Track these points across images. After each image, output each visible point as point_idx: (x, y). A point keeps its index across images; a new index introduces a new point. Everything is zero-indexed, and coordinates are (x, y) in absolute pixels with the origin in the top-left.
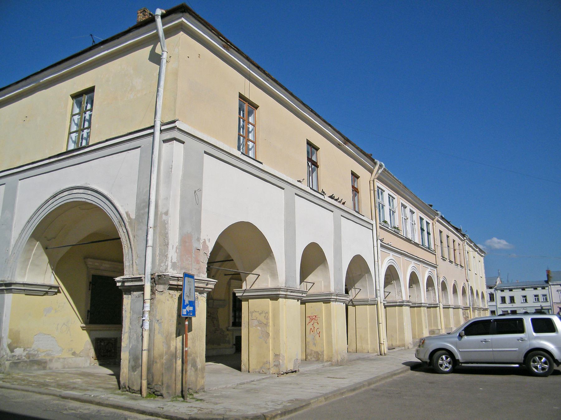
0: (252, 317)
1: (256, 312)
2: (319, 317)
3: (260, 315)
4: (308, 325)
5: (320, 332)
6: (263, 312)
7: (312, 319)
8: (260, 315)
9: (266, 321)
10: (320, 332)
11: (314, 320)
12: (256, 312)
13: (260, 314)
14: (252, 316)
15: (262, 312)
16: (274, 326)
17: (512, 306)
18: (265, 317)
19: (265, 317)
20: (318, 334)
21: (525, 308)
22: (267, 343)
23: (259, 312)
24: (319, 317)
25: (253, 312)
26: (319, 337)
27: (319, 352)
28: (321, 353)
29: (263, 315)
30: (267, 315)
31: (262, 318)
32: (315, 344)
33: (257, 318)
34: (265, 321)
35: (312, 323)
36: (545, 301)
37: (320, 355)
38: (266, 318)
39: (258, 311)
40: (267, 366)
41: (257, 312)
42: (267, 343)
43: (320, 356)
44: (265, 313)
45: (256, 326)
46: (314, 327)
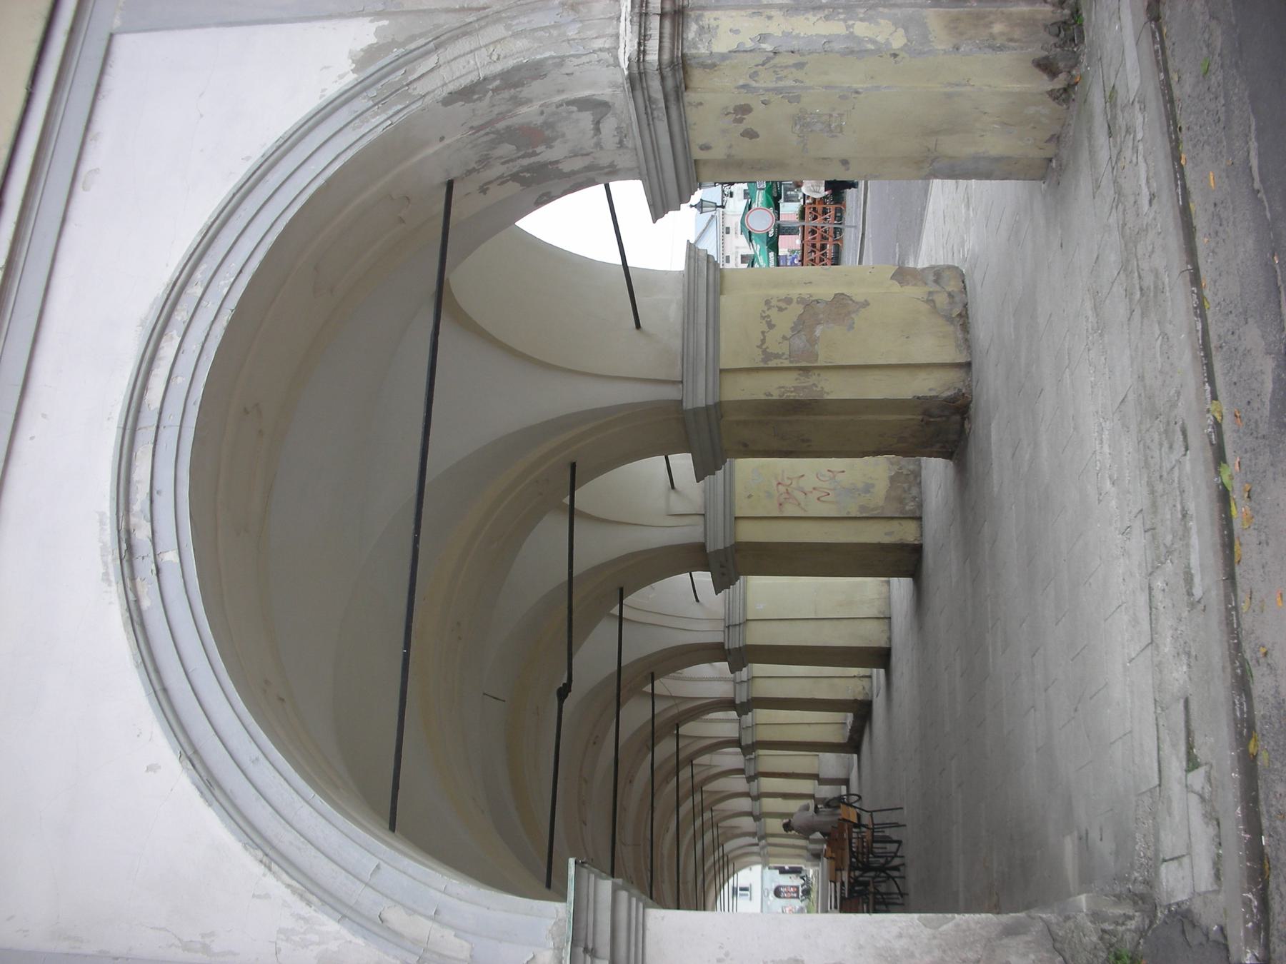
0: (783, 354)
1: (763, 341)
2: (783, 471)
3: (774, 326)
4: (805, 511)
5: (829, 471)
6: (764, 315)
7: (787, 496)
8: (774, 326)
9: (794, 304)
10: (829, 471)
11: (790, 490)
12: (763, 341)
13: (771, 326)
14: (777, 356)
15: (763, 318)
16: (810, 283)
18: (781, 309)
19: (781, 309)
20: (834, 476)
21: (766, 894)
22: (866, 301)
23: (765, 328)
24: (783, 471)
25: (764, 351)
26: (843, 472)
27: (893, 474)
28: (896, 468)
29: (773, 313)
30: (774, 302)
31: (784, 322)
32: (868, 488)
33: (784, 338)
34: (796, 310)
35: (800, 496)
36: (748, 893)
37: (901, 468)
38: (783, 305)
39: (763, 333)
40: (941, 300)
41: (764, 337)
42: (866, 301)
43: (905, 472)
44: (768, 309)
45: (813, 341)
46: (814, 489)
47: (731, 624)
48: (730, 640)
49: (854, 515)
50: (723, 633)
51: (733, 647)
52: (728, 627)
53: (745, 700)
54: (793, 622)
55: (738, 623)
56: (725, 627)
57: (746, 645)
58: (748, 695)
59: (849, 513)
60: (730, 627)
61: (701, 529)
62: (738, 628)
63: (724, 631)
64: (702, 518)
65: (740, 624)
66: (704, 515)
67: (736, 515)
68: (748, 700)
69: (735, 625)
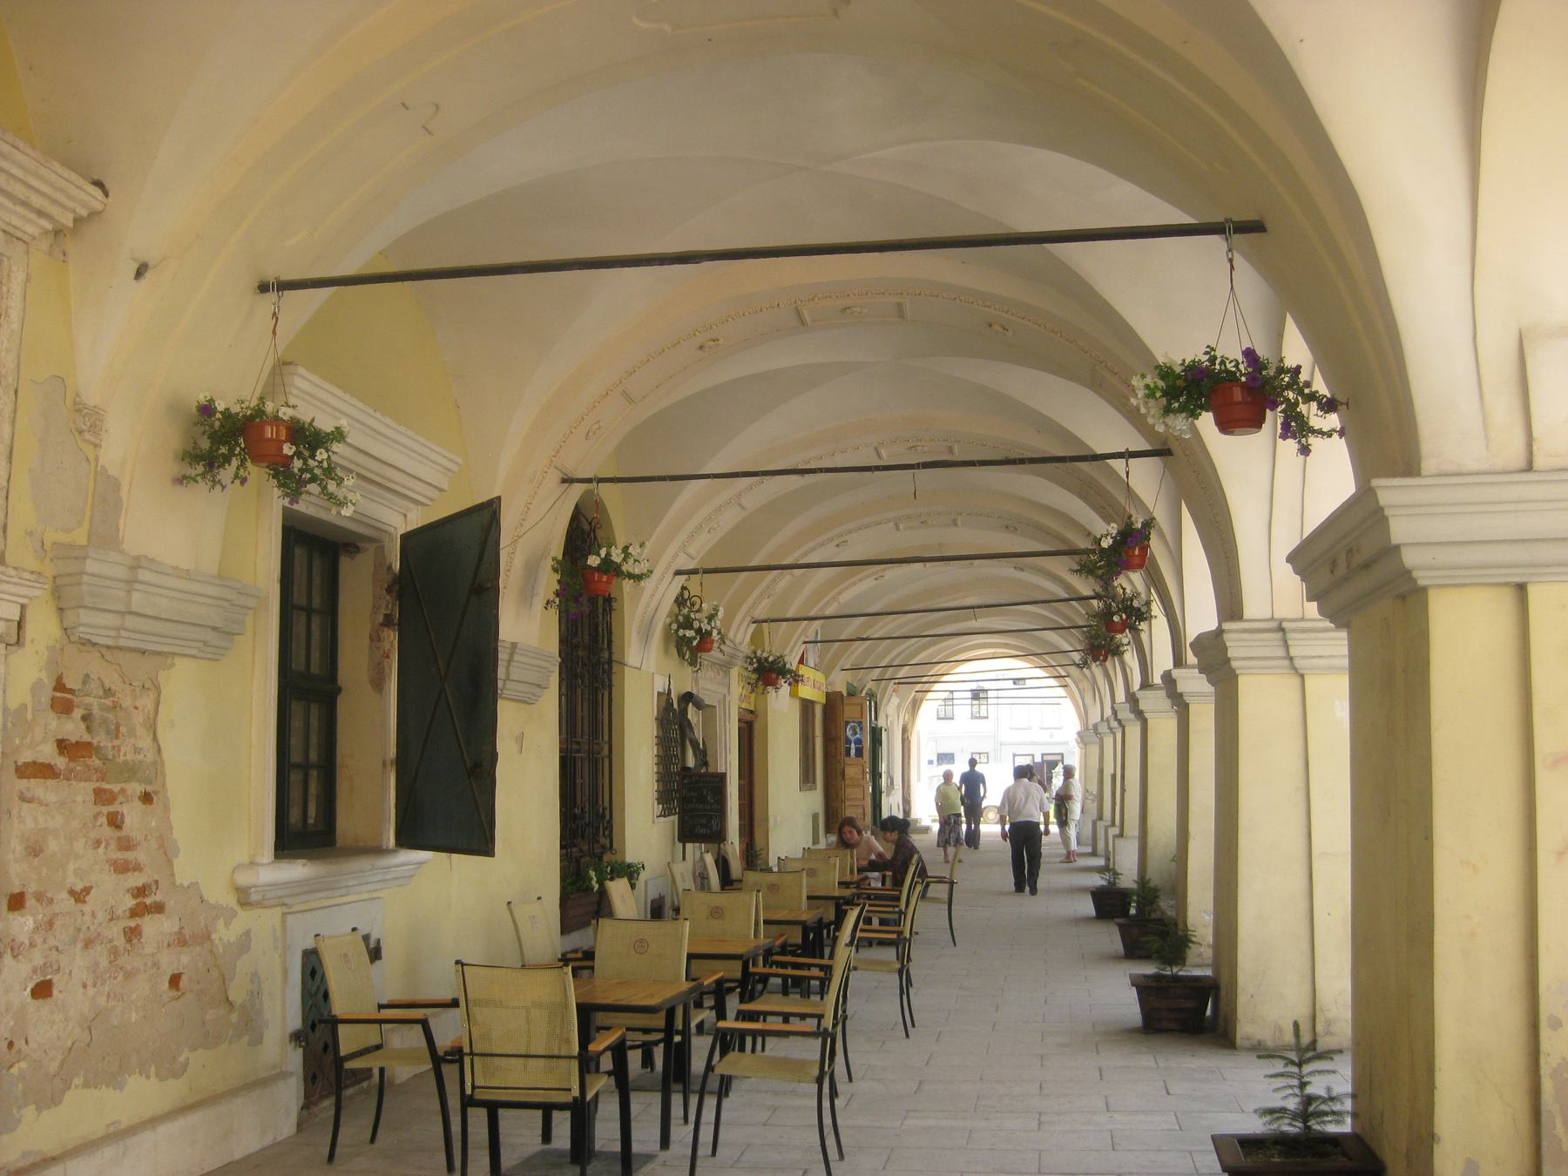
17: (1051, 736)
47: (1289, 636)
48: (1246, 636)
49: (1546, 1044)
50: (1269, 615)
51: (1228, 645)
52: (1281, 629)
53: (1179, 690)
54: (1301, 797)
55: (1293, 652)
56: (1281, 621)
57: (1236, 676)
58: (1194, 695)
59: (1556, 1024)
60: (1280, 635)
61: (1472, 456)
62: (1281, 652)
63: (1272, 619)
64: (1519, 460)
65: (1291, 659)
66: (1529, 467)
67: (1531, 589)
68: (1181, 695)
69: (1287, 647)
